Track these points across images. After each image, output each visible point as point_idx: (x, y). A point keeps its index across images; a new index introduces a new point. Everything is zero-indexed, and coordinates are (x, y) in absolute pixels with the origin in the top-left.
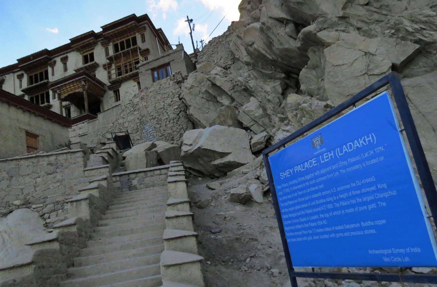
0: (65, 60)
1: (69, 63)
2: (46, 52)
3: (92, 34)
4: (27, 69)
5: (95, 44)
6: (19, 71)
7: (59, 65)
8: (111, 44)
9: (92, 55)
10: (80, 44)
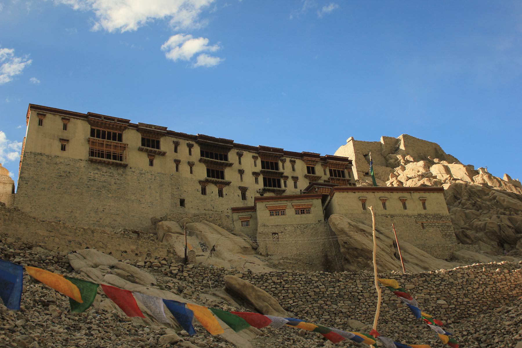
0: (293, 162)
1: (296, 166)
2: (281, 150)
3: (317, 156)
4: (262, 155)
5: (317, 162)
6: (256, 153)
7: (288, 164)
8: (328, 168)
9: (313, 169)
10: (309, 158)
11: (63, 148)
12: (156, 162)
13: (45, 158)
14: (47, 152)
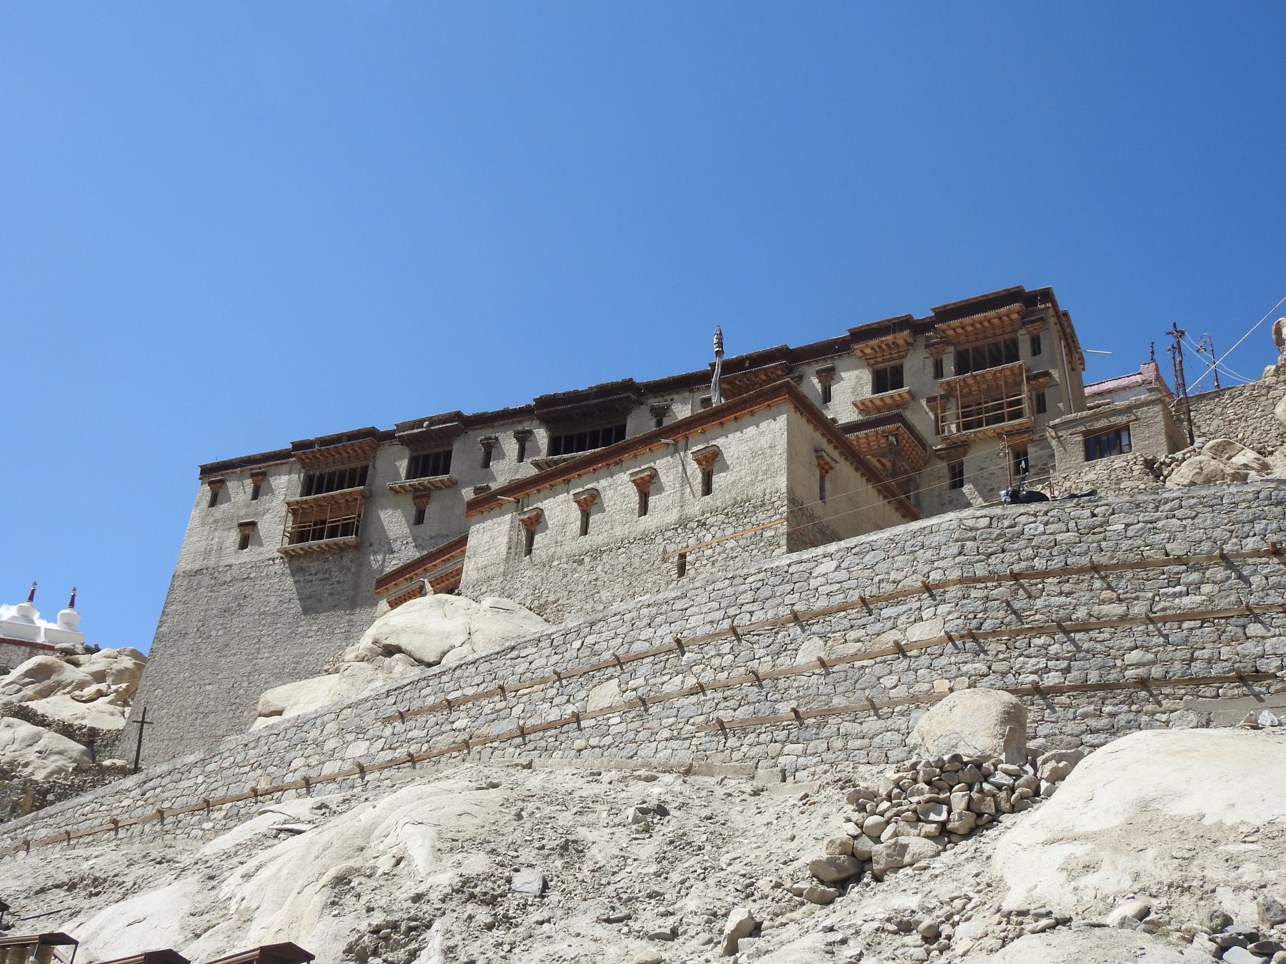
11: (244, 544)
12: (432, 510)
13: (206, 580)
14: (212, 562)
